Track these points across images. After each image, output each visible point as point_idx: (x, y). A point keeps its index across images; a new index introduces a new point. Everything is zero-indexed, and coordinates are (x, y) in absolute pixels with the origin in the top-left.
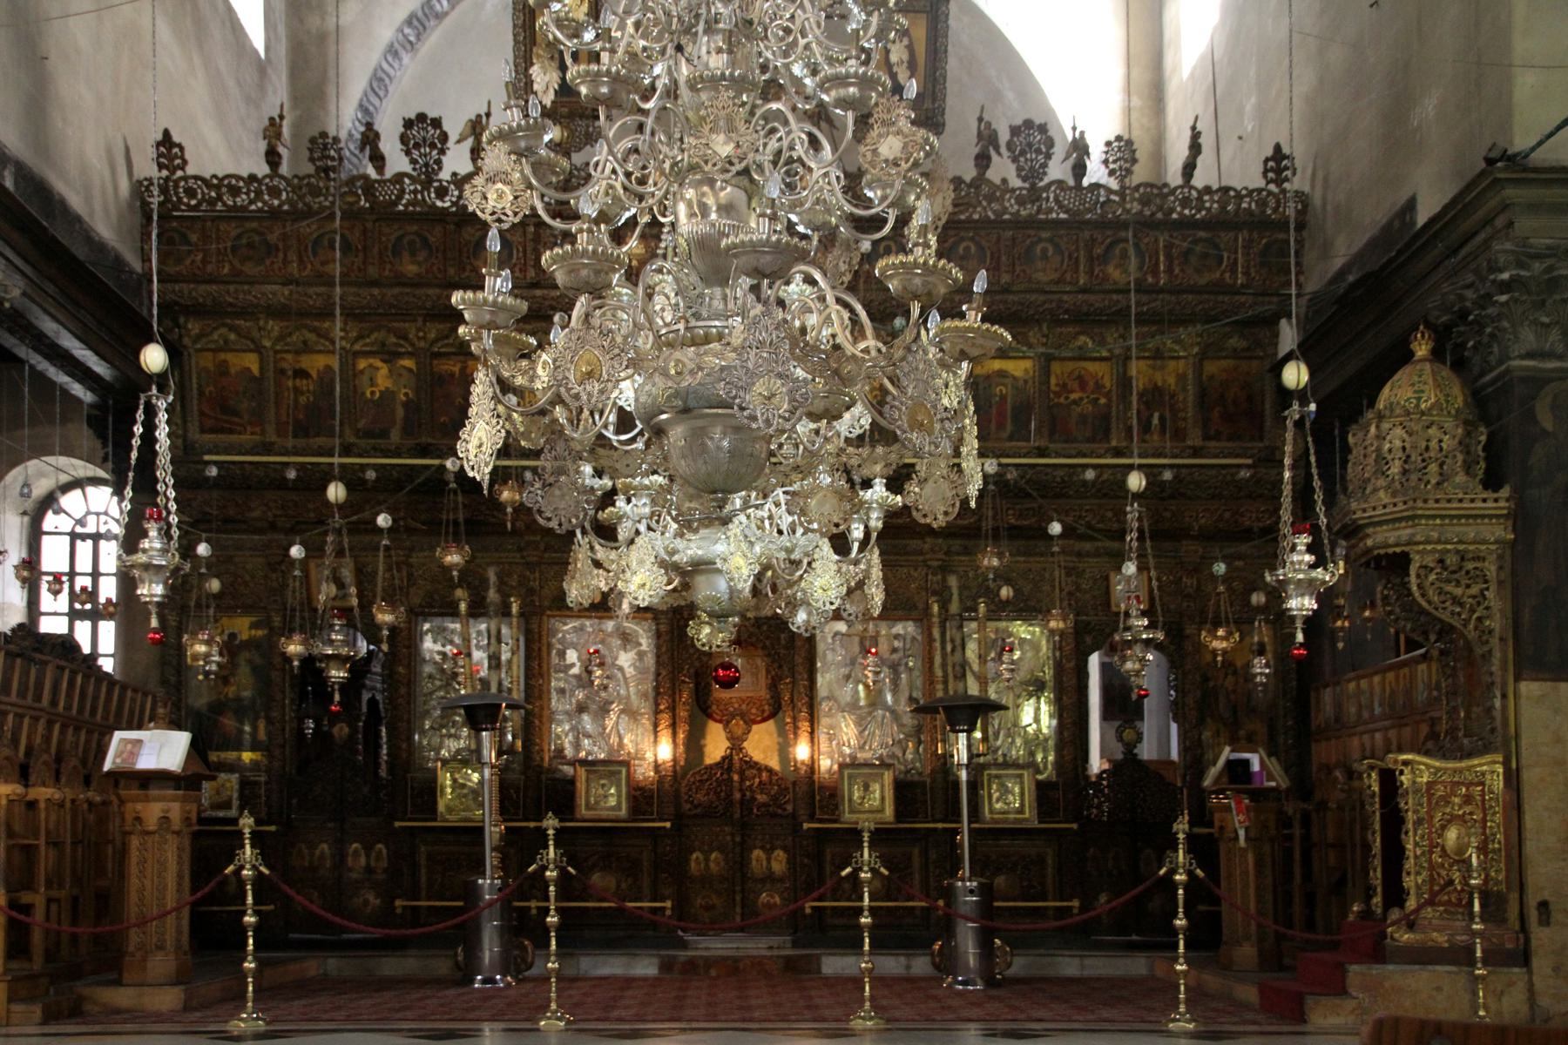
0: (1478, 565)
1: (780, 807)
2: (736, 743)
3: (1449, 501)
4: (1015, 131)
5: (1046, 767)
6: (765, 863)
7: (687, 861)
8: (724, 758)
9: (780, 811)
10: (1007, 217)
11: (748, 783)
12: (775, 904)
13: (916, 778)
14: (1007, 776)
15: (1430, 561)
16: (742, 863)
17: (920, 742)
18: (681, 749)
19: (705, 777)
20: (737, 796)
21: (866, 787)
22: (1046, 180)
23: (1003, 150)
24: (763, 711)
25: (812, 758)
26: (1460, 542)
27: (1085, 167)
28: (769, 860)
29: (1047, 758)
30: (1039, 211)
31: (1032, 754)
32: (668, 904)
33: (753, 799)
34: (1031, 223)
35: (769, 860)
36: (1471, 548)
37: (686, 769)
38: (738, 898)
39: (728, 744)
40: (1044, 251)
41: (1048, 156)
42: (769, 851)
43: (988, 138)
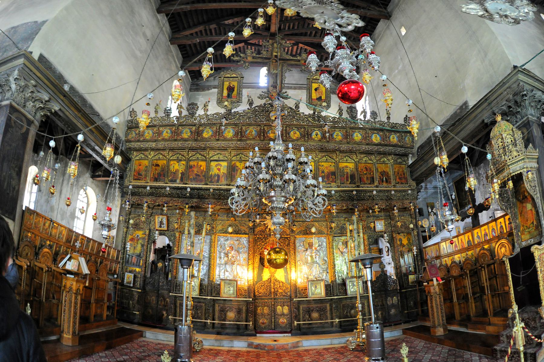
6: (281, 310)
7: (257, 310)
12: (285, 322)
16: (275, 311)
20: (273, 290)
28: (282, 309)
32: (251, 323)
33: (278, 291)
35: (282, 309)
37: (257, 283)
38: (273, 320)
42: (283, 306)
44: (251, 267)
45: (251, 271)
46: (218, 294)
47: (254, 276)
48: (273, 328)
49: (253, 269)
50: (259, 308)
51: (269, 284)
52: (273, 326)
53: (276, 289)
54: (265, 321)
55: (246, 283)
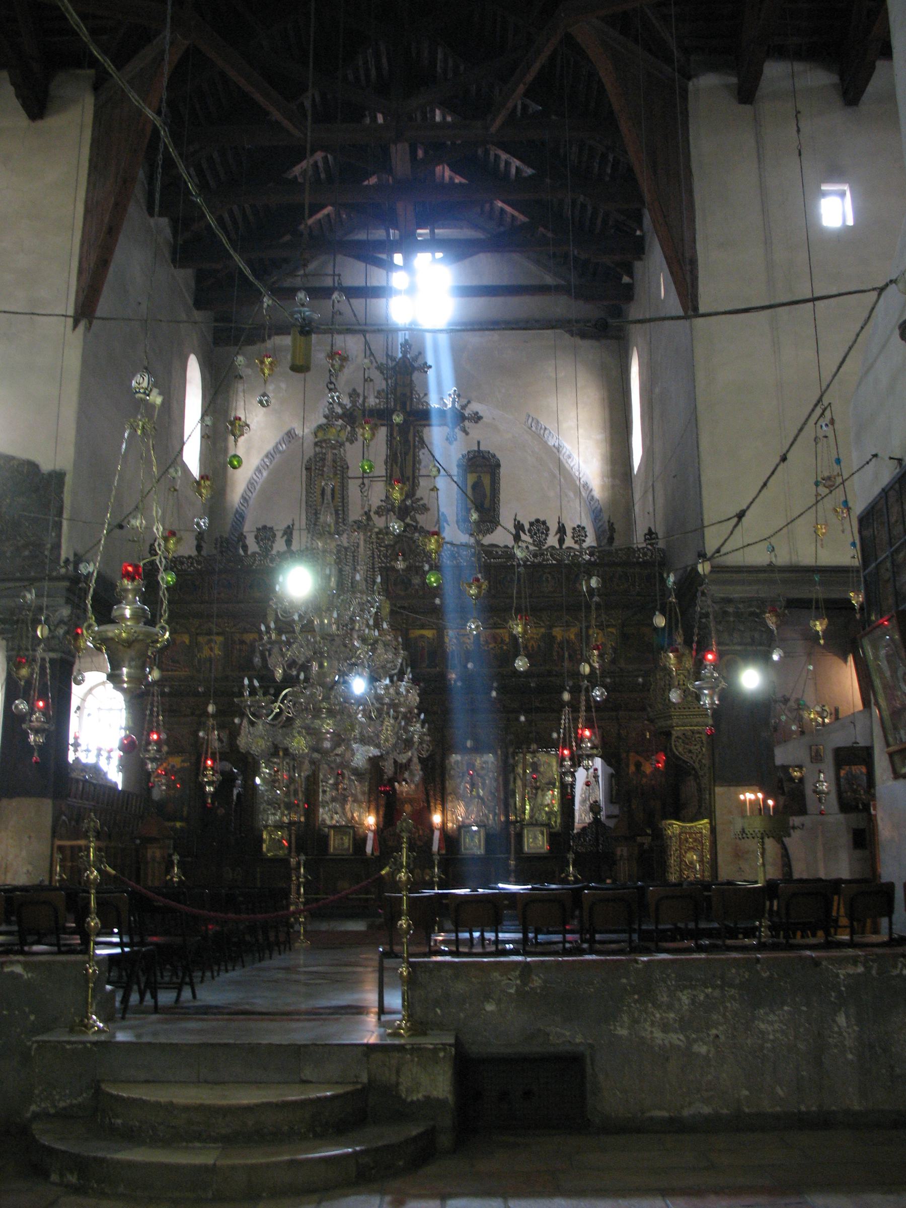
0: (698, 735)
3: (684, 708)
4: (531, 524)
5: (556, 826)
10: (529, 563)
15: (679, 734)
18: (381, 819)
22: (546, 546)
23: (527, 532)
26: (691, 726)
27: (564, 539)
29: (556, 822)
30: (544, 560)
31: (549, 819)
34: (540, 564)
36: (695, 728)
40: (547, 579)
41: (547, 535)
43: (519, 527)
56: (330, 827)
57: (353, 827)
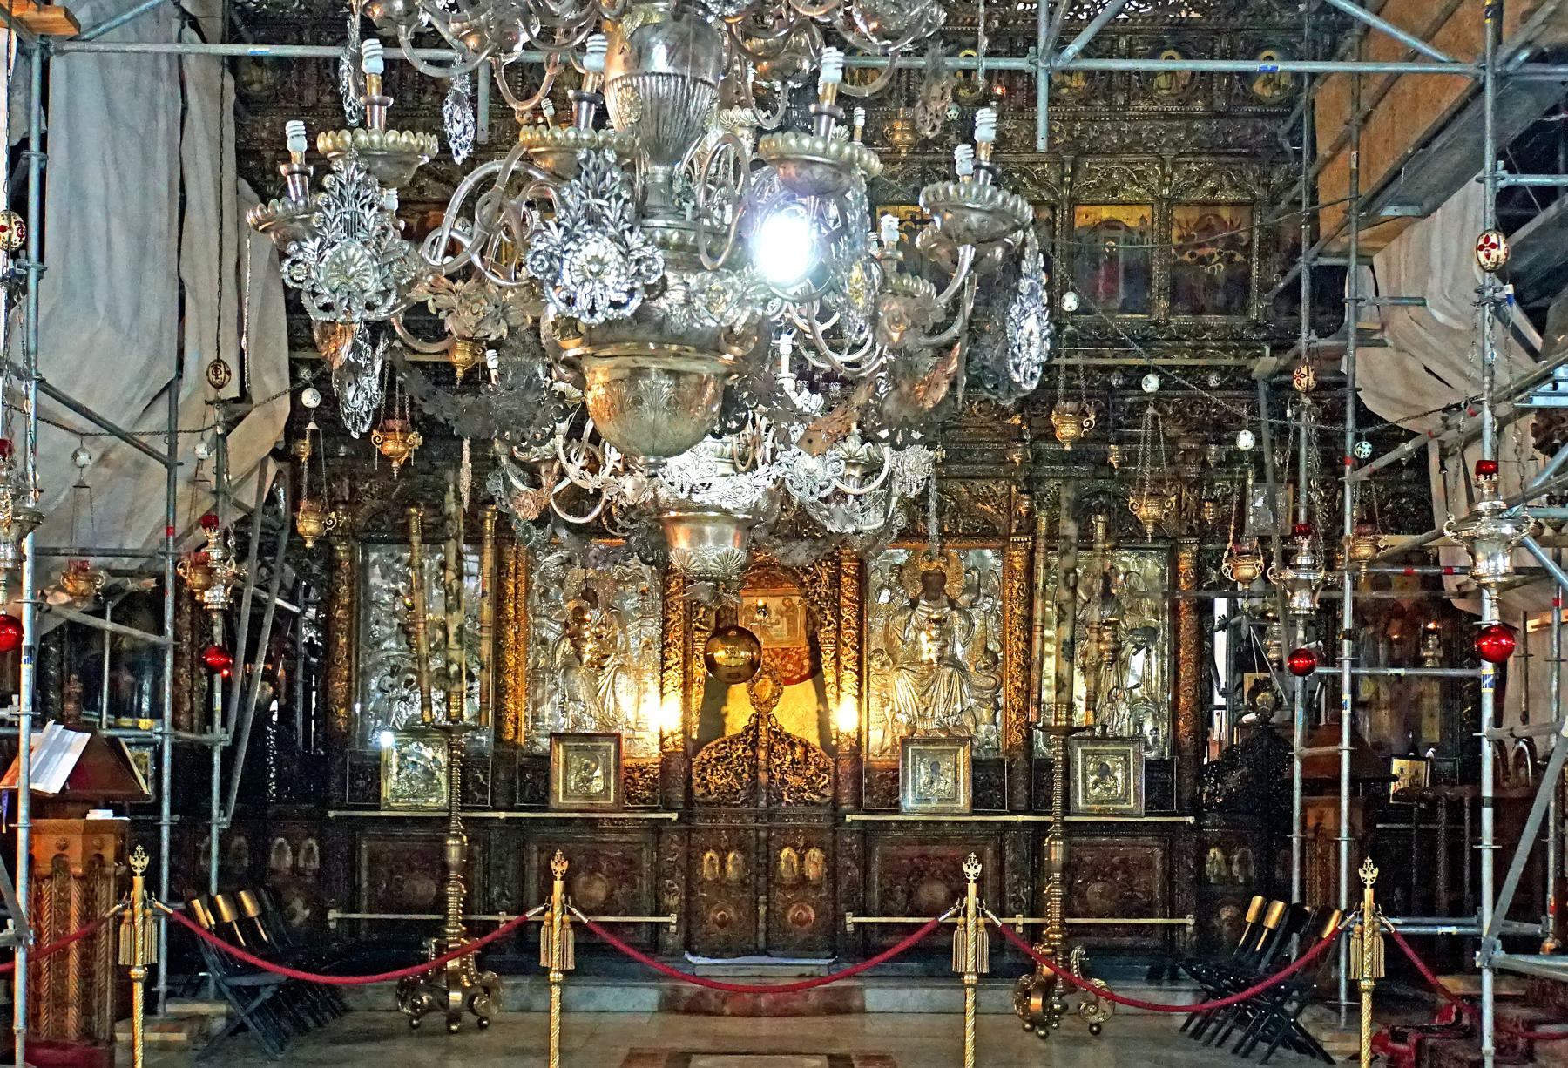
1: (816, 792)
2: (763, 709)
8: (747, 729)
9: (816, 798)
11: (778, 762)
13: (992, 756)
14: (1108, 753)
17: (997, 708)
19: (723, 753)
21: (935, 767)
24: (802, 667)
25: (860, 730)
28: (801, 859)
33: (784, 782)
35: (801, 859)
37: (699, 745)
39: (752, 710)
44: (674, 677)
45: (675, 698)
46: (540, 795)
47: (686, 722)
48: (762, 945)
49: (686, 686)
50: (708, 855)
51: (749, 753)
52: (761, 937)
53: (778, 776)
54: (731, 914)
55: (656, 749)
56: (556, 737)
57: (617, 738)
